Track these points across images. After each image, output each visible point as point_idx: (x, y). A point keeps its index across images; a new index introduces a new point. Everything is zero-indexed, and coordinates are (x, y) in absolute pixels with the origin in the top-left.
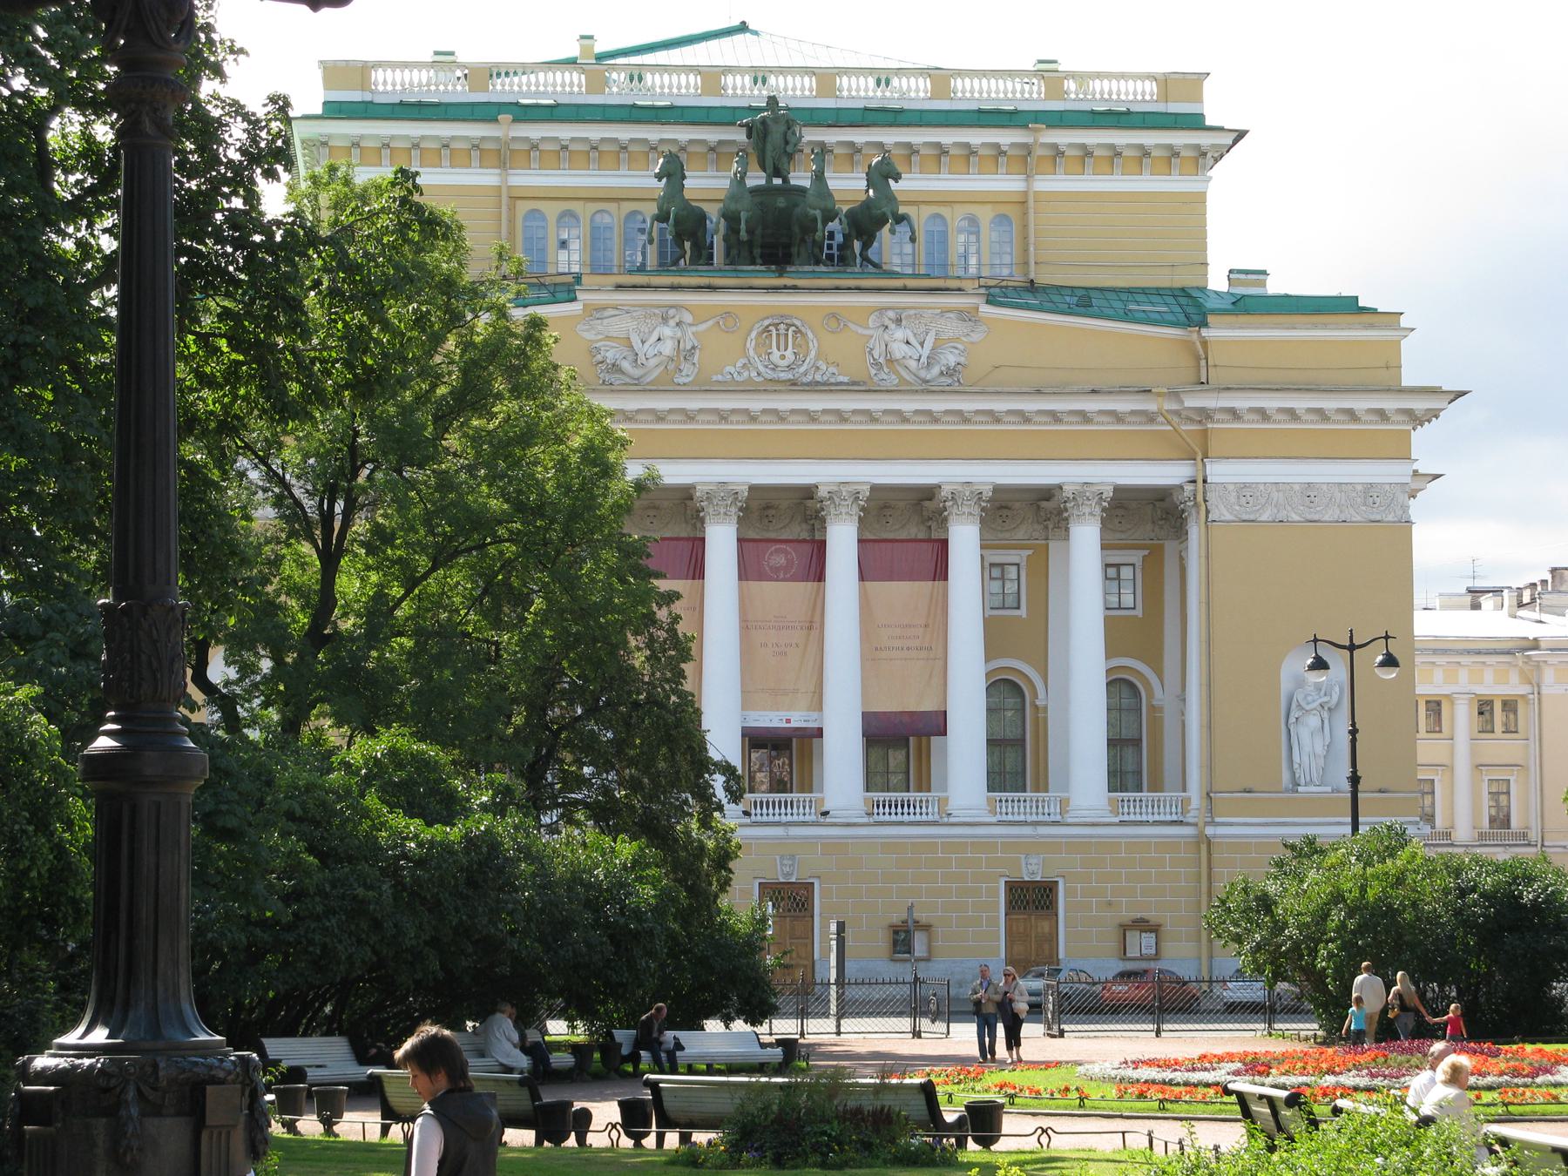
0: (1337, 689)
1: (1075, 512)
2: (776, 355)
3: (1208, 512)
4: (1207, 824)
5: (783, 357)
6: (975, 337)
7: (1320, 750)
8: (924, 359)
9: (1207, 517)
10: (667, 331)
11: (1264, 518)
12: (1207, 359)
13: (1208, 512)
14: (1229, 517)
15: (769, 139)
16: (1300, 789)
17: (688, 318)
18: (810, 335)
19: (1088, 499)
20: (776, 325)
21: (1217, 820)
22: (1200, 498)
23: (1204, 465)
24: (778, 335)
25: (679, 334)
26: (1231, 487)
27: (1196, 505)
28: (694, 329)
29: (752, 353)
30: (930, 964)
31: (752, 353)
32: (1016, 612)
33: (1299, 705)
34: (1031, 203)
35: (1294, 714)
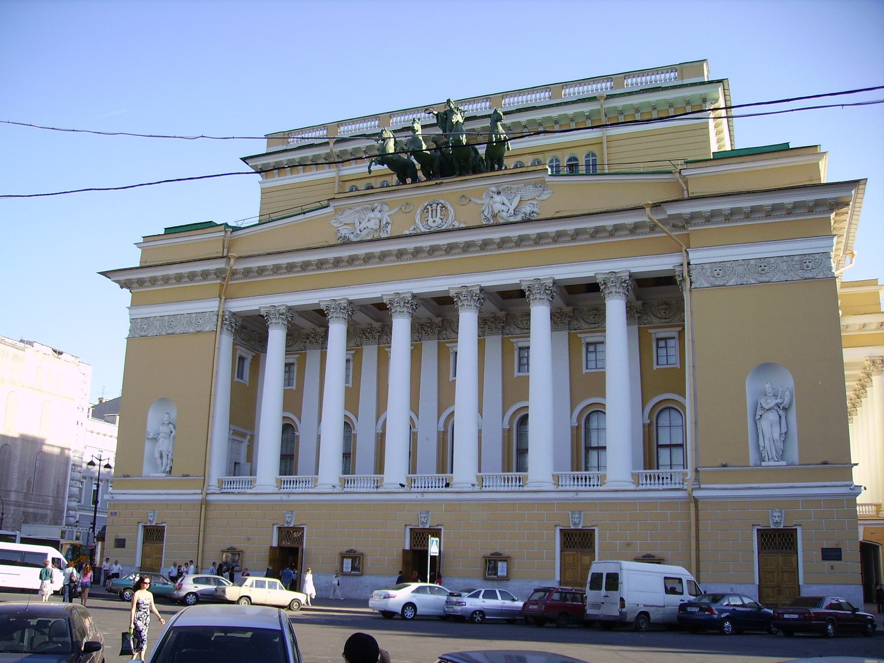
0: (788, 393)
1: (607, 291)
2: (431, 220)
5: (434, 221)
6: (544, 197)
7: (776, 435)
10: (372, 215)
11: (731, 283)
12: (687, 190)
13: (691, 283)
14: (706, 285)
16: (763, 464)
17: (386, 208)
20: (431, 205)
21: (702, 486)
22: (685, 274)
24: (432, 210)
26: (707, 266)
27: (683, 280)
29: (417, 221)
30: (509, 583)
33: (762, 407)
34: (605, 145)
35: (759, 413)
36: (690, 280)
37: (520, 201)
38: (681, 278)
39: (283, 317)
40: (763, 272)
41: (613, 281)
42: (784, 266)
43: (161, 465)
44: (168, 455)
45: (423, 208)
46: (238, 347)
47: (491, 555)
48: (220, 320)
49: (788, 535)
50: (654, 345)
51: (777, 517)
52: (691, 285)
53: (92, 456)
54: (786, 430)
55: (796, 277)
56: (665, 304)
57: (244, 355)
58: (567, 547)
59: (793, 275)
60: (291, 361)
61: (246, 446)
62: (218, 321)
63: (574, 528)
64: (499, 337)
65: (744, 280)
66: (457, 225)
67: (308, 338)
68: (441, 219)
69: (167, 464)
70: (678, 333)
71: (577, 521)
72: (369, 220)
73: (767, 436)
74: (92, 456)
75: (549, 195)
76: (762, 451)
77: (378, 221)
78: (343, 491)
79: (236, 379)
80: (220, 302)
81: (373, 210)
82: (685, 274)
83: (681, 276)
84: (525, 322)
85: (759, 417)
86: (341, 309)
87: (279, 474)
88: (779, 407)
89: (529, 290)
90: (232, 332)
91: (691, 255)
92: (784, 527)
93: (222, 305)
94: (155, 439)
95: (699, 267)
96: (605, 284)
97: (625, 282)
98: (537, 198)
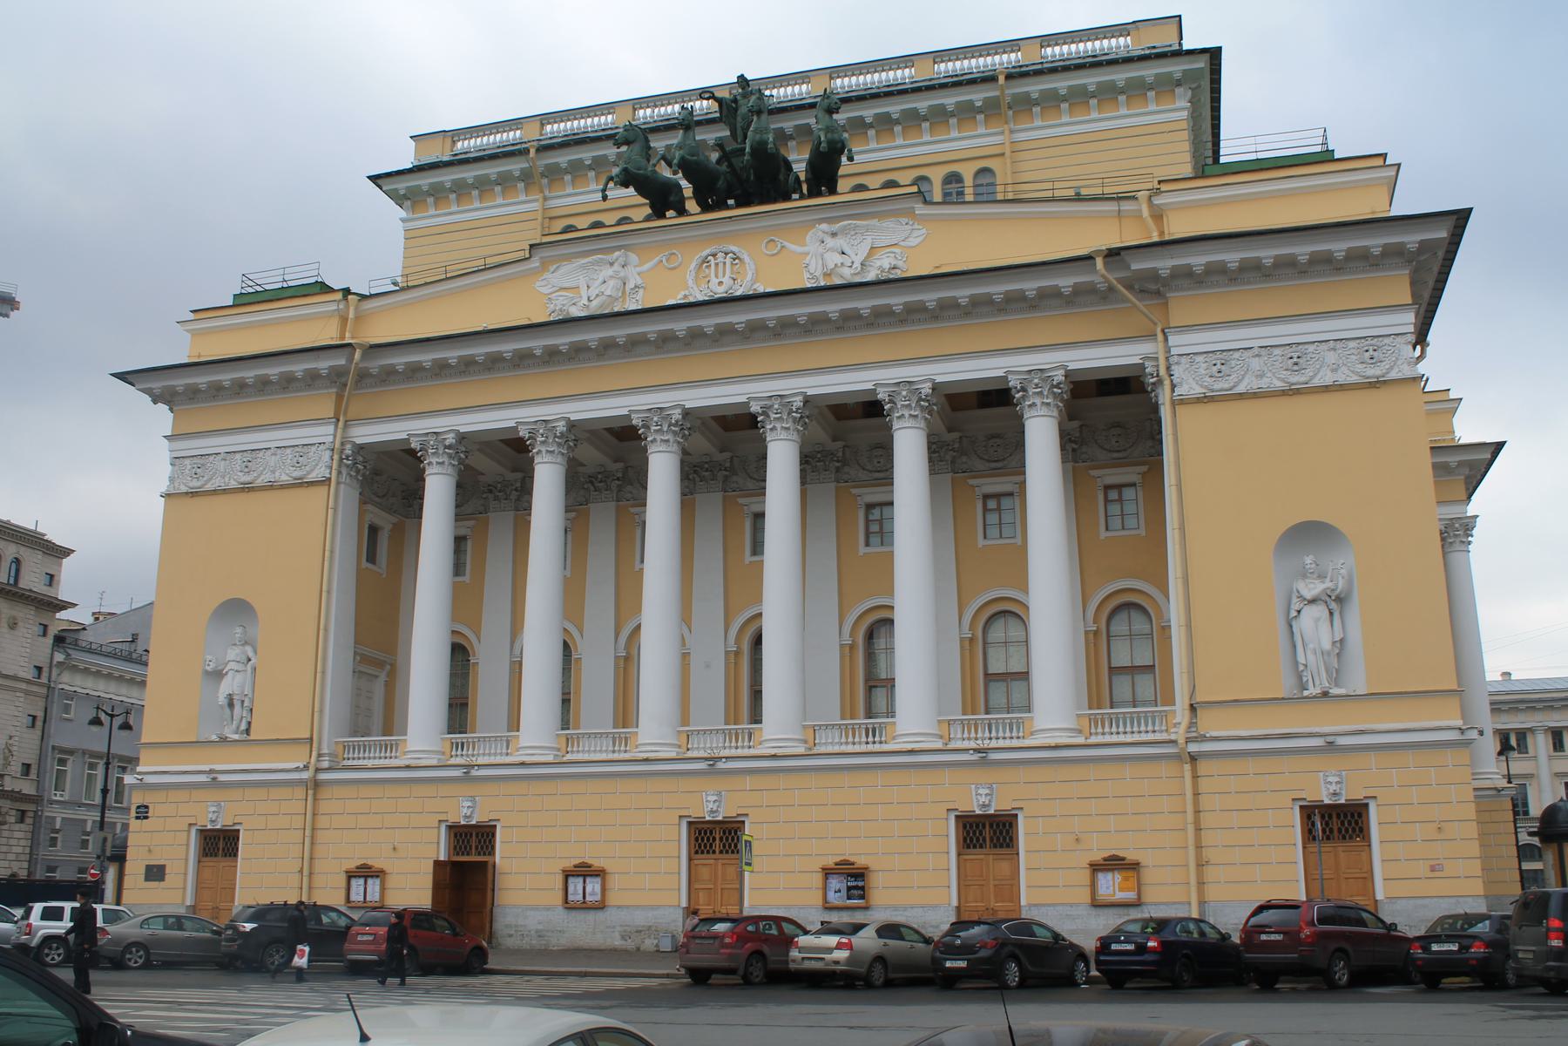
2: (714, 281)
3: (1173, 387)
4: (1188, 740)
5: (721, 283)
7: (1327, 645)
8: (857, 265)
9: (1173, 391)
10: (609, 271)
13: (1173, 387)
14: (1197, 390)
15: (739, 112)
17: (633, 257)
18: (745, 257)
19: (1037, 386)
20: (714, 255)
22: (1162, 372)
23: (1166, 339)
24: (717, 264)
25: (622, 274)
27: (1160, 382)
28: (638, 269)
29: (690, 283)
31: (690, 283)
32: (1012, 541)
35: (1296, 605)
36: (1172, 381)
37: (872, 248)
38: (1155, 379)
39: (451, 451)
40: (1296, 368)
41: (1036, 385)
42: (1331, 358)
43: (229, 719)
44: (243, 702)
45: (700, 260)
46: (370, 507)
47: (836, 864)
48: (336, 457)
49: (1352, 816)
50: (1101, 497)
51: (1334, 784)
52: (1173, 391)
53: (98, 708)
54: (1342, 636)
55: (1351, 375)
56: (1118, 426)
57: (377, 521)
58: (968, 847)
59: (1347, 372)
60: (462, 532)
61: (383, 683)
62: (333, 460)
63: (981, 812)
64: (833, 485)
65: (1264, 384)
66: (761, 290)
67: (491, 491)
68: (734, 280)
69: (242, 717)
70: (1140, 476)
71: (983, 799)
72: (605, 282)
73: (1311, 646)
74: (98, 708)
75: (921, 238)
76: (1302, 671)
77: (620, 283)
78: (565, 759)
79: (365, 564)
80: (336, 426)
81: (612, 264)
82: (1162, 372)
83: (1155, 375)
84: (875, 461)
85: (1295, 614)
86: (556, 437)
87: (446, 730)
88: (1330, 596)
89: (891, 401)
90: (358, 480)
91: (1172, 340)
92: (1346, 800)
93: (339, 431)
94: (218, 675)
95: (1183, 360)
96: (1023, 389)
97: (1057, 386)
98: (902, 243)
